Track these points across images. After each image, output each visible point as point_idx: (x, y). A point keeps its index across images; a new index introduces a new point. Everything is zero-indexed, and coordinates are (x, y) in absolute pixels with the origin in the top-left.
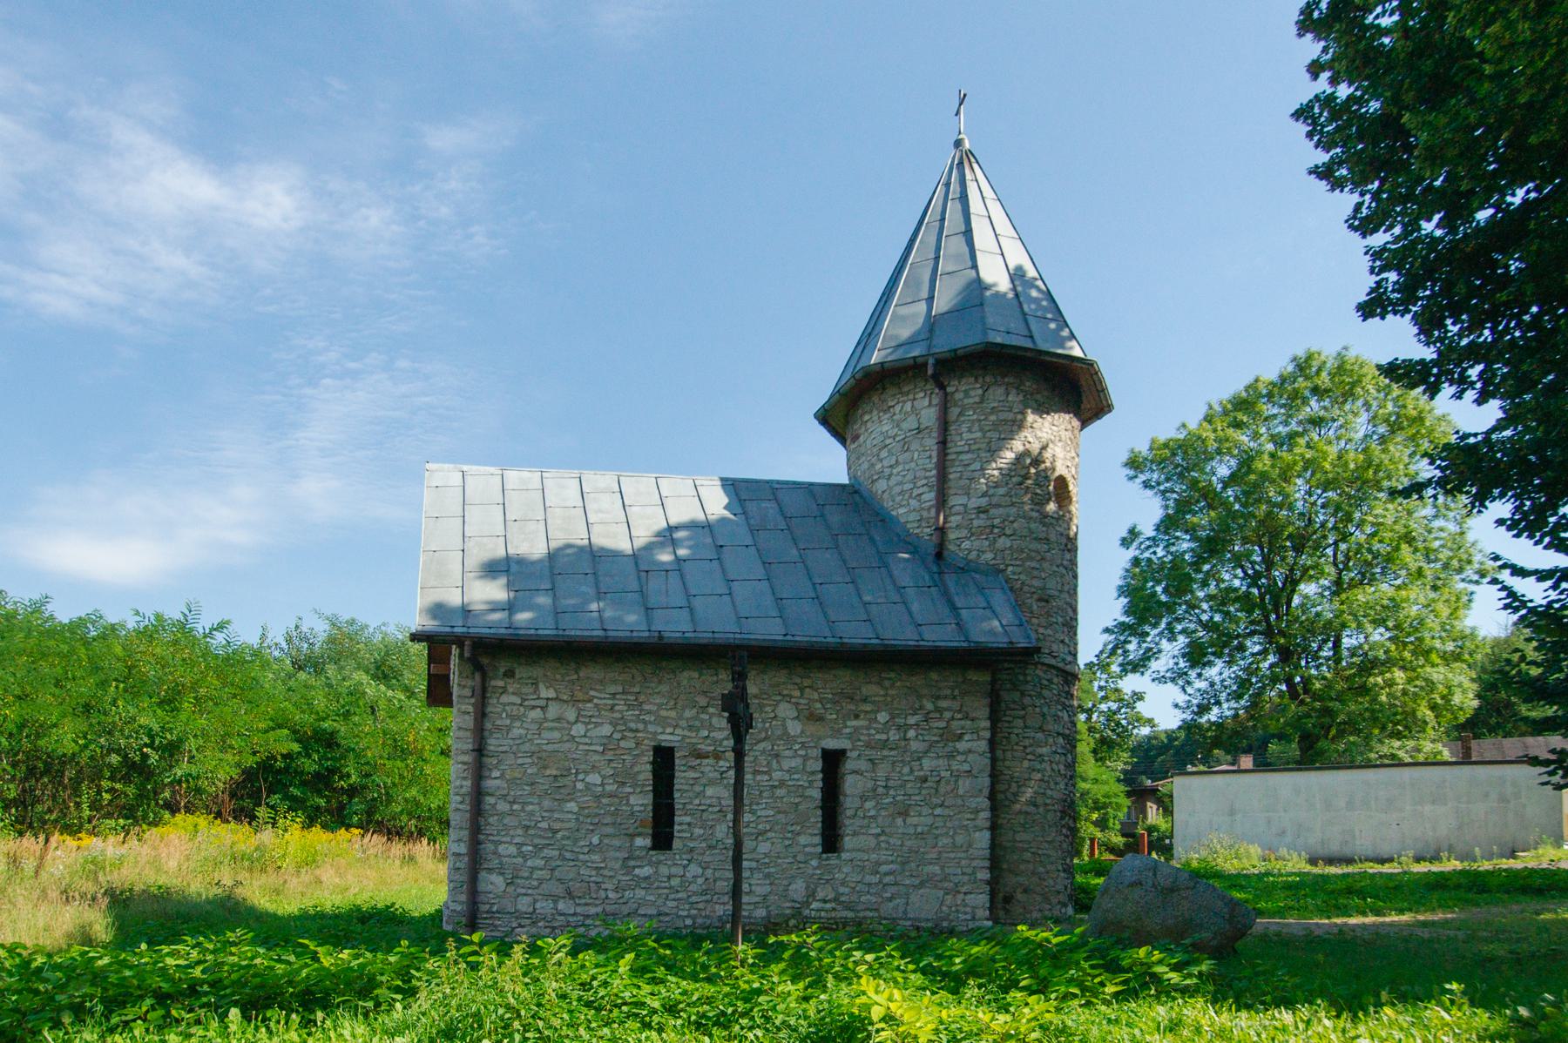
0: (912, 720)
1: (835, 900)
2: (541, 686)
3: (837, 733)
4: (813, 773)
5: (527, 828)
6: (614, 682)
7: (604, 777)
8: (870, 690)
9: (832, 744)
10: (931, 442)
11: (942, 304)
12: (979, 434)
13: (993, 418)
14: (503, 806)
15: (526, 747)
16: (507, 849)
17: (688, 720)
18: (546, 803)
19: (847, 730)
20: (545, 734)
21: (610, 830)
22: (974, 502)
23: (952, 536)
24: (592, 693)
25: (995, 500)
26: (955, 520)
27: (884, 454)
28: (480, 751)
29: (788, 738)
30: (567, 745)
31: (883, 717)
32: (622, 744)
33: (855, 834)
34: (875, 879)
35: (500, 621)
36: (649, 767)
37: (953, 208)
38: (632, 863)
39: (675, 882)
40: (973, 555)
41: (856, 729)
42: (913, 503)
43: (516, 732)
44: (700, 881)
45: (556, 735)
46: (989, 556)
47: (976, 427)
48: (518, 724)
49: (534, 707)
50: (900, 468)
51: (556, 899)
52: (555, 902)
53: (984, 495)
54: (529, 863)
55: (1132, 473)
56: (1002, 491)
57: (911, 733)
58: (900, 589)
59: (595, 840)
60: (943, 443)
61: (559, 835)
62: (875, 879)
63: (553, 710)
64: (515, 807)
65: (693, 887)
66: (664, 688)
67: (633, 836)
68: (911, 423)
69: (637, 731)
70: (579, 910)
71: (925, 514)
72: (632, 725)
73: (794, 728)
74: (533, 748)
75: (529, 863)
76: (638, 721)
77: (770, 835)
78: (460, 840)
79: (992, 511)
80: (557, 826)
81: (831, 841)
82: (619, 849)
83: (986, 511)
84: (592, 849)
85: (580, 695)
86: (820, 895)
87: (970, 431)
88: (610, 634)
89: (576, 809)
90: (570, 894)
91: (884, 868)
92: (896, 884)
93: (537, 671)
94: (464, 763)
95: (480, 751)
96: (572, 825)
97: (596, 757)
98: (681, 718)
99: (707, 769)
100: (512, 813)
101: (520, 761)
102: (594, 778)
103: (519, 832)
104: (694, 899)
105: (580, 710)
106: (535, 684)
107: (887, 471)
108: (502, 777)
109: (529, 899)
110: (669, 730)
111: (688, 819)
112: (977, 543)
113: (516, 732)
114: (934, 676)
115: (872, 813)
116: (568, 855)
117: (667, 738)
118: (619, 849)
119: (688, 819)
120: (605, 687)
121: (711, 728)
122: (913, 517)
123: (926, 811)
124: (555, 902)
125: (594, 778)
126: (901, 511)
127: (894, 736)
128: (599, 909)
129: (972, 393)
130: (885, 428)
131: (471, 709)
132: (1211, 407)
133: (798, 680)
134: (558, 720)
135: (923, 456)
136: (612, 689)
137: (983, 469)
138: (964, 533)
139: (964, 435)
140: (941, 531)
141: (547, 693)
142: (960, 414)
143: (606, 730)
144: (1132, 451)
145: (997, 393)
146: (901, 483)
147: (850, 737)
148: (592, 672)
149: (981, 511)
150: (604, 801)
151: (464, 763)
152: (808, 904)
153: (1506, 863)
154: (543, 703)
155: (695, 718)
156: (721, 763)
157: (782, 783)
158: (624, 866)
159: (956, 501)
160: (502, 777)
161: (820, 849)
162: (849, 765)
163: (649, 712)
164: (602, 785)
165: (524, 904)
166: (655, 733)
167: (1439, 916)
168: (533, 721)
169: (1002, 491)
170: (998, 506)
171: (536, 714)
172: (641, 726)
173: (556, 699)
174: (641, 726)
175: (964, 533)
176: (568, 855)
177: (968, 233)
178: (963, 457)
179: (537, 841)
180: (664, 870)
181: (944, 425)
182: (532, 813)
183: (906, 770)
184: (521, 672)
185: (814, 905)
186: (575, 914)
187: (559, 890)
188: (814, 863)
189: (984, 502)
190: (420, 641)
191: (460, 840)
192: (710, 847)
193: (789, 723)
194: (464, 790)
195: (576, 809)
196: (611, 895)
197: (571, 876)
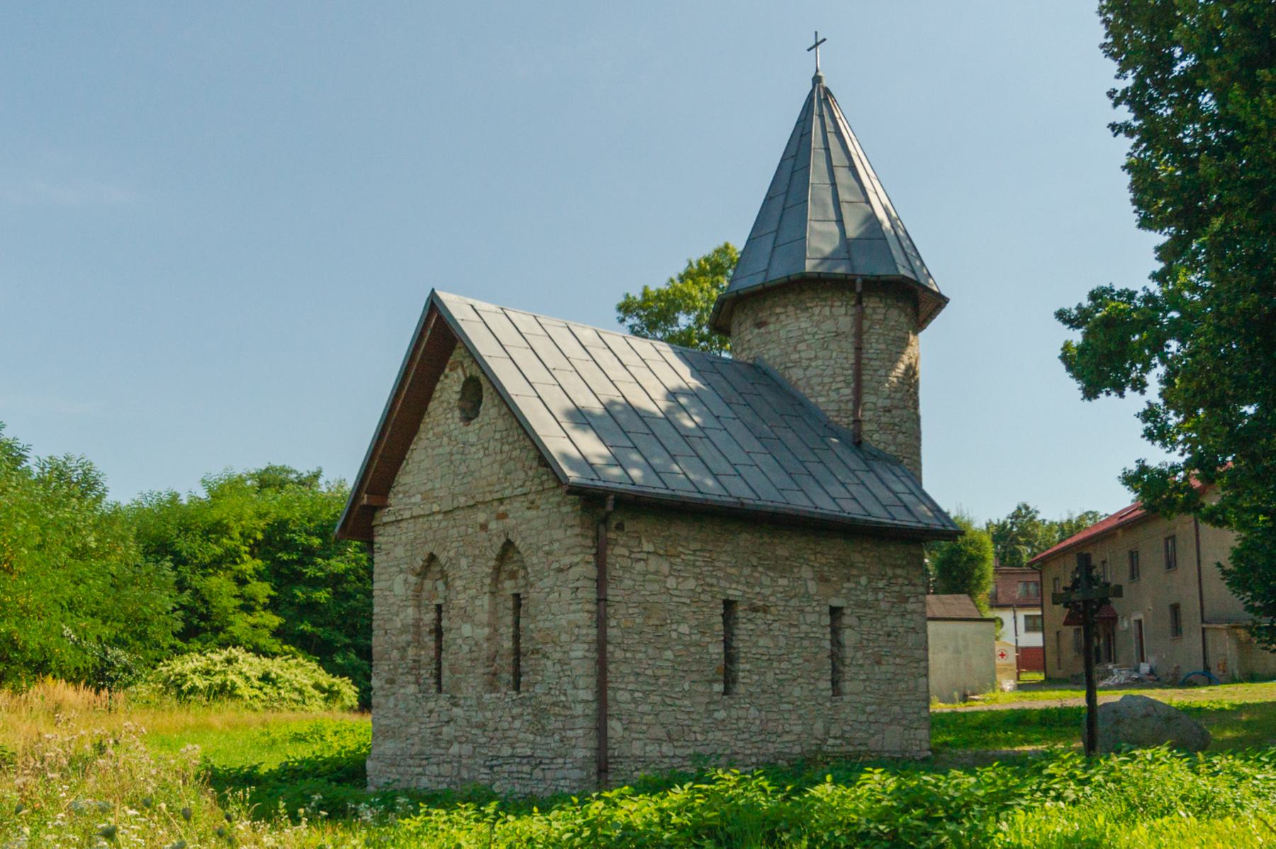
0: (881, 584)
1: (842, 737)
2: (643, 540)
3: (837, 593)
4: (824, 627)
5: (638, 674)
6: (695, 540)
7: (691, 627)
8: (857, 558)
9: (836, 602)
10: (848, 346)
11: (852, 230)
12: (883, 346)
13: (892, 334)
14: (619, 654)
15: (635, 598)
16: (623, 696)
17: (746, 577)
18: (650, 651)
19: (844, 591)
20: (649, 587)
21: (695, 677)
22: (881, 403)
23: (866, 427)
24: (680, 549)
25: (895, 402)
26: (868, 415)
27: (802, 347)
28: (602, 600)
29: (807, 596)
30: (664, 597)
31: (864, 581)
32: (703, 597)
33: (852, 680)
34: (863, 718)
35: (616, 477)
36: (721, 619)
37: (832, 139)
38: (712, 707)
39: (742, 724)
40: (881, 446)
41: (850, 589)
42: (833, 395)
43: (628, 583)
44: (758, 722)
45: (656, 587)
46: (892, 448)
47: (881, 340)
48: (628, 575)
49: (638, 560)
50: (820, 362)
51: (659, 741)
52: (660, 745)
53: (888, 397)
54: (640, 709)
55: (621, 315)
56: (899, 395)
57: (881, 596)
58: (853, 471)
59: (686, 687)
60: (859, 349)
61: (661, 681)
62: (863, 718)
63: (653, 563)
64: (628, 655)
65: (754, 729)
66: (728, 547)
67: (711, 682)
68: (829, 326)
69: (712, 585)
70: (678, 752)
71: (843, 405)
72: (709, 580)
73: (812, 587)
74: (641, 599)
75: (640, 709)
76: (712, 576)
77: (800, 680)
78: (587, 688)
79: (894, 412)
80: (659, 673)
81: (836, 690)
82: (703, 694)
83: (889, 411)
84: (686, 694)
85: (672, 551)
86: (832, 733)
87: (877, 342)
88: (709, 497)
89: (672, 657)
90: (670, 738)
91: (868, 709)
92: (876, 722)
93: (641, 526)
94: (588, 612)
95: (602, 600)
96: (669, 672)
97: (685, 609)
98: (741, 575)
99: (759, 622)
100: (626, 660)
101: (631, 611)
102: (684, 628)
103: (632, 678)
104: (754, 739)
105: (672, 564)
106: (639, 538)
107: (805, 363)
108: (618, 626)
109: (642, 743)
110: (734, 586)
111: (748, 667)
112: (884, 437)
113: (628, 583)
114: (892, 548)
115: (861, 662)
116: (668, 701)
117: (734, 592)
118: (703, 694)
119: (748, 667)
120: (689, 542)
121: (761, 585)
122: (833, 406)
123: (891, 660)
124: (660, 745)
125: (684, 628)
126: (821, 400)
127: (870, 597)
128: (691, 751)
129: (879, 311)
130: (803, 325)
131: (591, 559)
132: (691, 264)
133: (812, 546)
134: (656, 573)
135: (843, 355)
136: (694, 546)
137: (887, 376)
138: (875, 427)
139: (874, 345)
140: (857, 422)
141: (647, 547)
142: (870, 327)
143: (691, 584)
144: (627, 296)
145: (894, 314)
146: (821, 376)
147: (847, 597)
148: (681, 529)
149: (887, 410)
150: (693, 649)
151: (588, 612)
152: (826, 740)
153: (961, 708)
154: (644, 556)
155: (751, 576)
156: (769, 617)
157: (807, 636)
158: (707, 710)
159: (868, 399)
160: (618, 626)
161: (830, 693)
162: (846, 620)
163: (720, 569)
164: (690, 634)
165: (637, 749)
166: (725, 588)
167: (1021, 748)
168: (639, 573)
169: (899, 395)
170: (897, 408)
171: (640, 566)
172: (714, 581)
173: (655, 553)
174: (714, 581)
175: (875, 427)
176: (668, 701)
177: (852, 168)
178: (872, 363)
179: (646, 688)
180: (734, 713)
181: (859, 334)
182: (640, 661)
183: (879, 626)
184: (629, 526)
185: (831, 741)
186: (674, 757)
187: (659, 732)
188: (828, 704)
189: (888, 403)
190: (575, 494)
191: (587, 688)
192: (764, 692)
193: (810, 583)
194: (589, 639)
195: (672, 657)
196: (699, 737)
197: (671, 719)
